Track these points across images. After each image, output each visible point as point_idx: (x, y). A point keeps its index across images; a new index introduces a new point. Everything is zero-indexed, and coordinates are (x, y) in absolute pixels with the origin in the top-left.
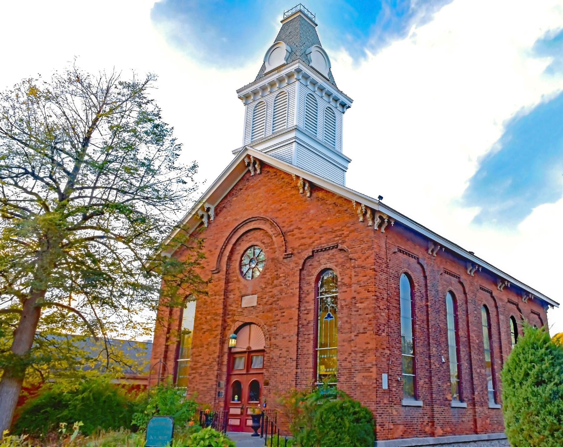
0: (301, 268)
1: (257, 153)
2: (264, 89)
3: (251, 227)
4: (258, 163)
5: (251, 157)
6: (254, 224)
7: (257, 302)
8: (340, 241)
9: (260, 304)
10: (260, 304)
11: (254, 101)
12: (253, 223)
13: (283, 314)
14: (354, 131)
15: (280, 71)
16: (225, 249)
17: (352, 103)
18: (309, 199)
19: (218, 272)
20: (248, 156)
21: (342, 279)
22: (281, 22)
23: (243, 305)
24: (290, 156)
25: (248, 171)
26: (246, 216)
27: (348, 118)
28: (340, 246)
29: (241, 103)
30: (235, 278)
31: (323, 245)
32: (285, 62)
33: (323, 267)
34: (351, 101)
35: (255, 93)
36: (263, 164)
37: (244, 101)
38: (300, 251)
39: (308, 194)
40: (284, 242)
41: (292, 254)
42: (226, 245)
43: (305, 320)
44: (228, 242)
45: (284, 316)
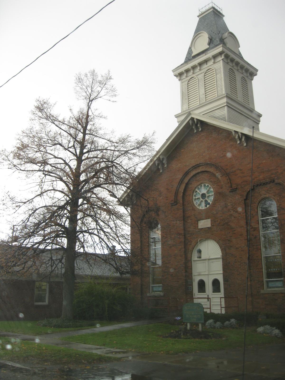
0: (245, 198)
1: (198, 115)
2: (194, 68)
3: (199, 171)
4: (199, 123)
5: (195, 119)
6: (202, 168)
7: (211, 224)
8: (276, 178)
9: (213, 226)
10: (213, 226)
11: (187, 77)
12: (201, 167)
13: (172, 187)
14: (262, 93)
15: (230, 51)
16: (179, 187)
17: (257, 72)
18: (245, 148)
19: (176, 205)
20: (192, 119)
21: (281, 205)
22: (198, 16)
23: (200, 227)
24: (216, 114)
25: (191, 130)
26: (193, 162)
27: (257, 83)
28: (276, 181)
29: (176, 80)
30: (191, 208)
31: (262, 181)
32: (208, 46)
33: (263, 196)
34: (257, 70)
35: (187, 71)
36: (202, 123)
37: (179, 78)
38: (243, 186)
39: (245, 145)
40: (229, 180)
41: (236, 189)
42: (180, 186)
43: (253, 235)
44: (182, 182)
45: (235, 233)
